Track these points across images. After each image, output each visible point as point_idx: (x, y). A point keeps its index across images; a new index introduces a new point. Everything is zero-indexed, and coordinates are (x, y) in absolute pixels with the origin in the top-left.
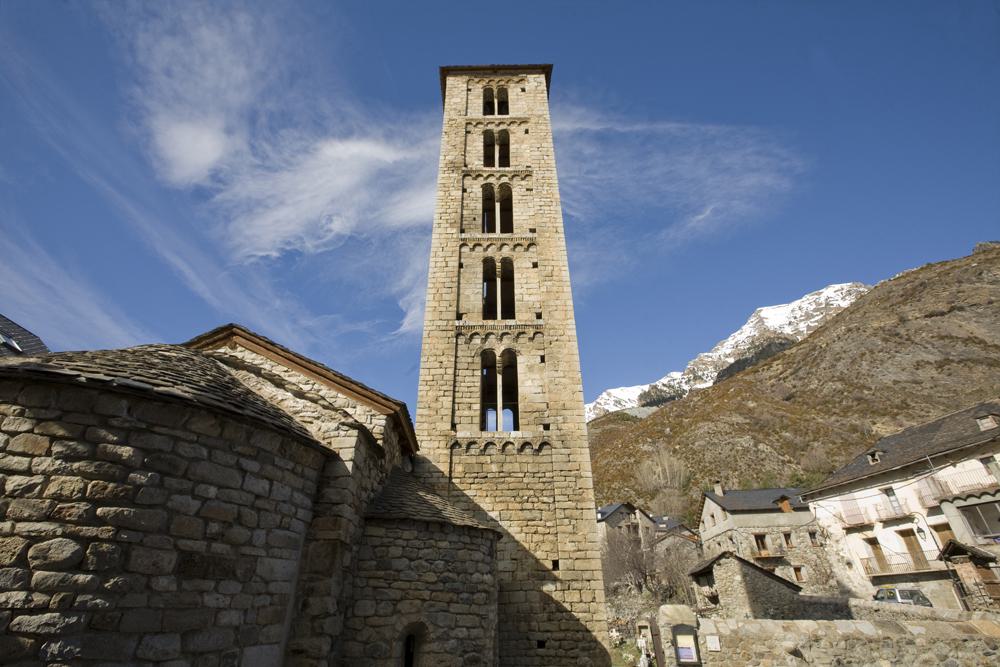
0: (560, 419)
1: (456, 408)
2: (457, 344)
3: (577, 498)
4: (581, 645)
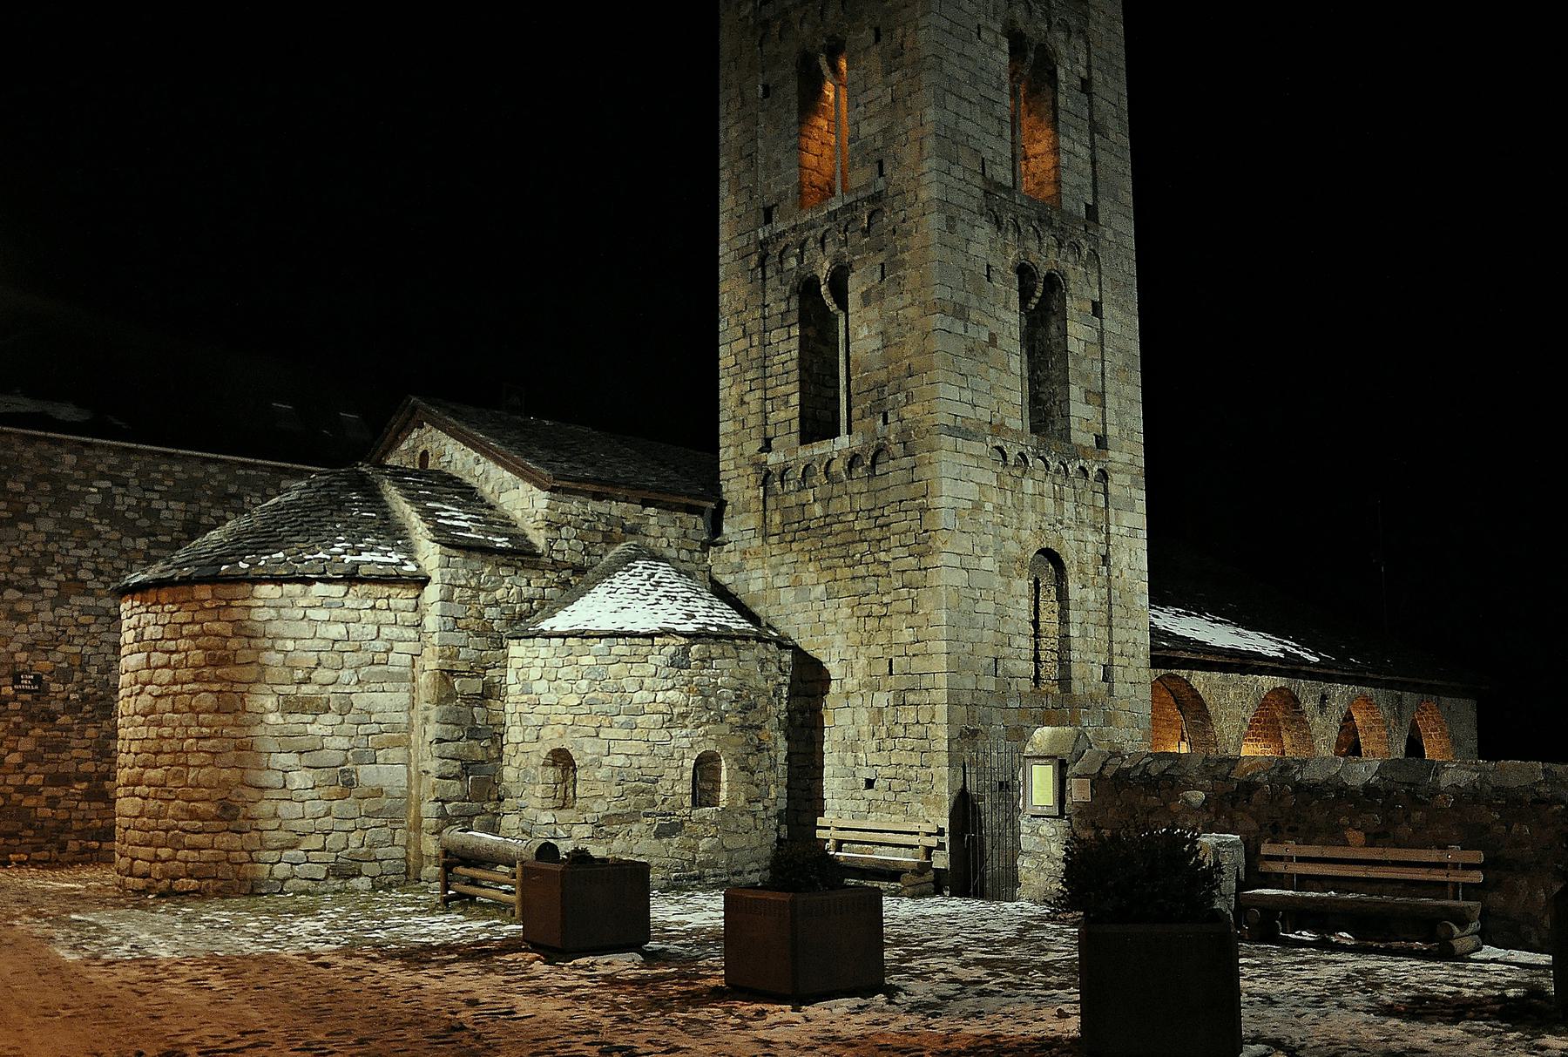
0: (901, 396)
1: (769, 408)
2: (764, 278)
3: (922, 548)
4: (914, 785)
